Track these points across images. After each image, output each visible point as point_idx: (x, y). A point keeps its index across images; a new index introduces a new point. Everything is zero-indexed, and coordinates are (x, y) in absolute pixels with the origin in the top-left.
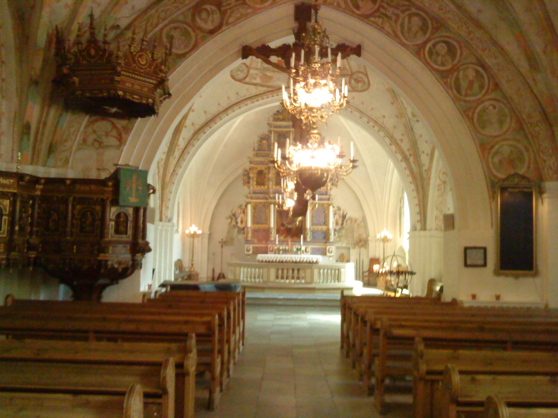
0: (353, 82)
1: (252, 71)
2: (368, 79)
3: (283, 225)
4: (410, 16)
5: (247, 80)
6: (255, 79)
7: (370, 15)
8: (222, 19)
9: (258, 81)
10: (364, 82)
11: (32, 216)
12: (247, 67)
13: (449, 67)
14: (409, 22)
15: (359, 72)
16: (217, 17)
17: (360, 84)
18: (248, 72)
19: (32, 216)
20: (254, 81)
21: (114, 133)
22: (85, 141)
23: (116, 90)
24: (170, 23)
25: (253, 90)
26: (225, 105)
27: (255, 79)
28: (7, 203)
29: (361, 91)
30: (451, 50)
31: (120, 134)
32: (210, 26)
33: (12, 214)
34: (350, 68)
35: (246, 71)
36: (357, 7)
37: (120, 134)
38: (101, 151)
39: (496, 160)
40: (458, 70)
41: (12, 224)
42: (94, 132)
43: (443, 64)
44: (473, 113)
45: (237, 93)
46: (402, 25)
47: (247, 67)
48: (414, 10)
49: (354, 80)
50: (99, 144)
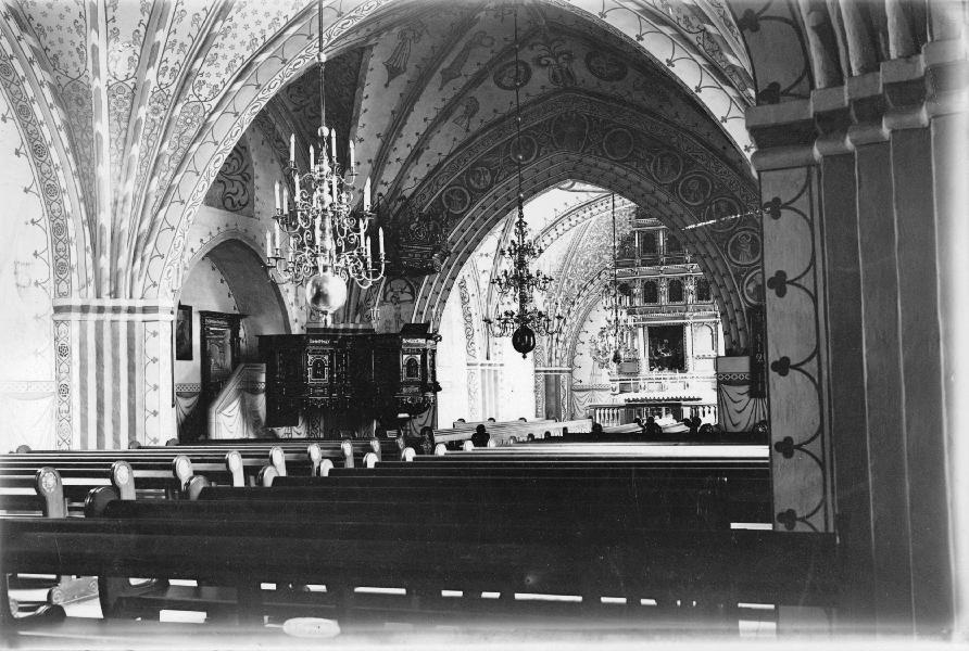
3: (657, 354)
4: (663, 156)
7: (626, 160)
8: (493, 177)
11: (346, 365)
13: (700, 202)
14: (662, 162)
16: (488, 178)
19: (346, 365)
21: (408, 289)
22: (385, 297)
23: (401, 260)
24: (449, 186)
26: (552, 218)
28: (326, 358)
30: (704, 185)
31: (412, 290)
32: (482, 186)
33: (331, 365)
36: (613, 154)
37: (412, 290)
38: (398, 306)
39: (751, 288)
40: (711, 204)
41: (331, 373)
42: (392, 290)
43: (696, 201)
44: (727, 244)
46: (655, 167)
48: (666, 151)
50: (397, 301)
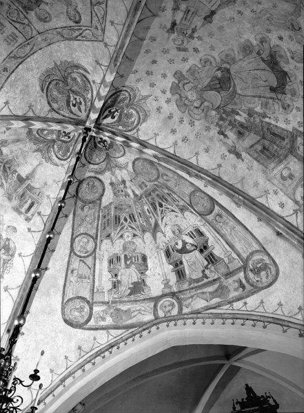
0: (251, 275)
1: (96, 309)
2: (269, 255)
5: (92, 323)
6: (103, 319)
9: (109, 321)
10: (265, 267)
12: (88, 302)
15: (252, 254)
17: (263, 273)
18: (91, 309)
20: (102, 323)
25: (103, 338)
27: (103, 319)
29: (270, 285)
34: (239, 255)
35: (87, 308)
45: (80, 348)
47: (88, 302)
49: (251, 270)
